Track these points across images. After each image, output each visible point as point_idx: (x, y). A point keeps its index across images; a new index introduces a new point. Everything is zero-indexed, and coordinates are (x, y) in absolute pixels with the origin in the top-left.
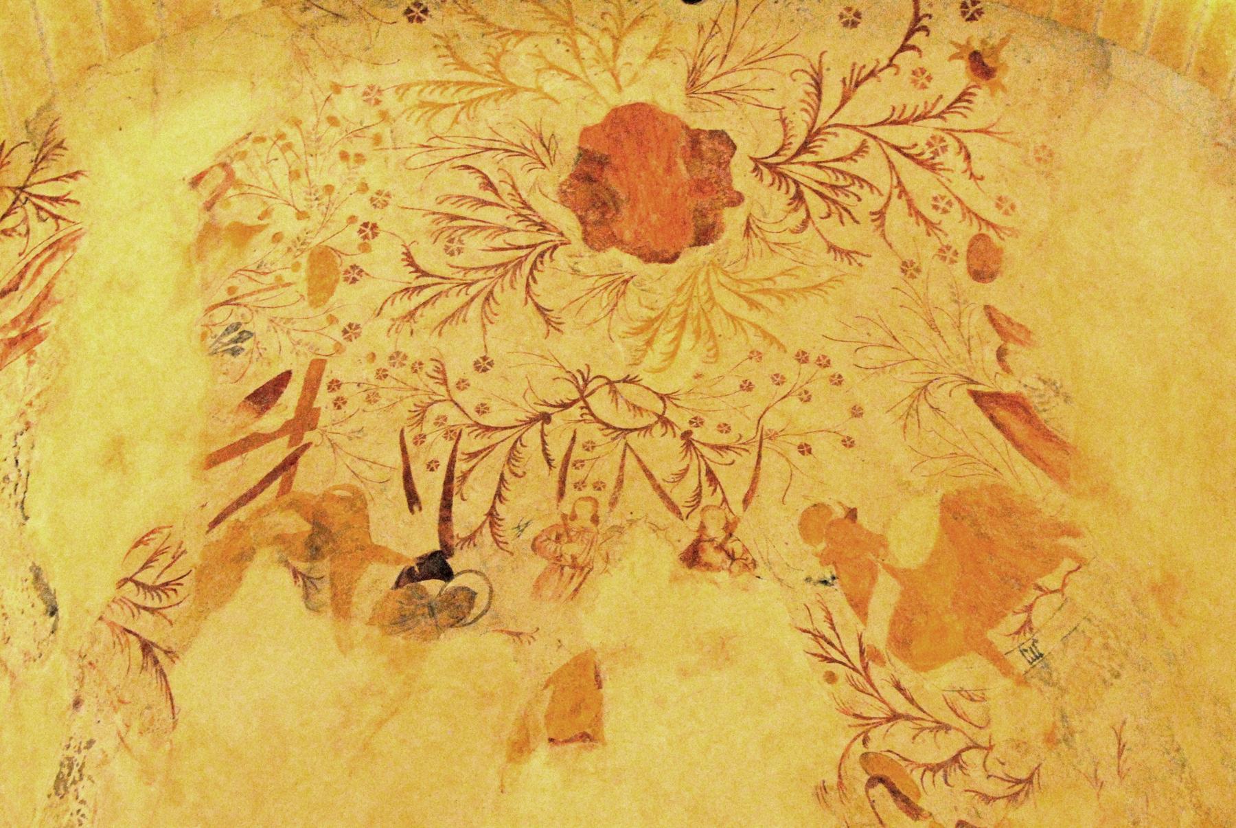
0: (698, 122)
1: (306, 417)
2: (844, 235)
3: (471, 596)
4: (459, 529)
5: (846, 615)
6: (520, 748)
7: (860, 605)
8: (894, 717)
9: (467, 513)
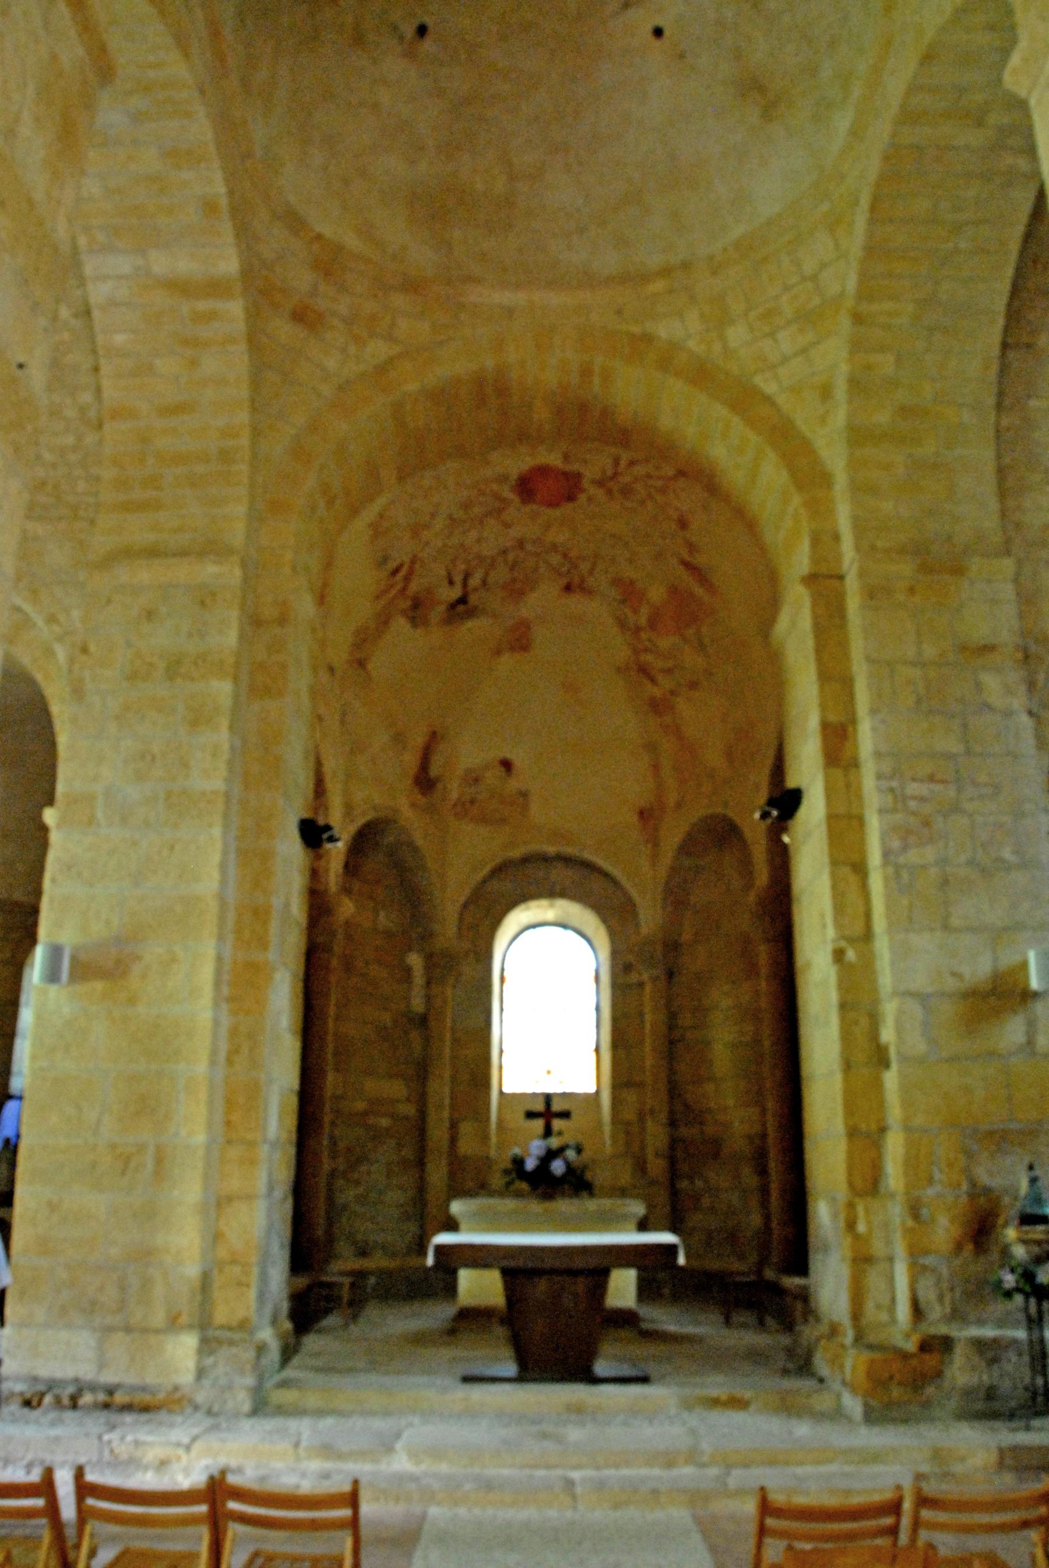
0: (568, 468)
1: (411, 572)
2: (629, 504)
3: (476, 608)
4: (470, 588)
5: (630, 614)
6: (498, 652)
7: (635, 611)
8: (646, 650)
9: (475, 581)
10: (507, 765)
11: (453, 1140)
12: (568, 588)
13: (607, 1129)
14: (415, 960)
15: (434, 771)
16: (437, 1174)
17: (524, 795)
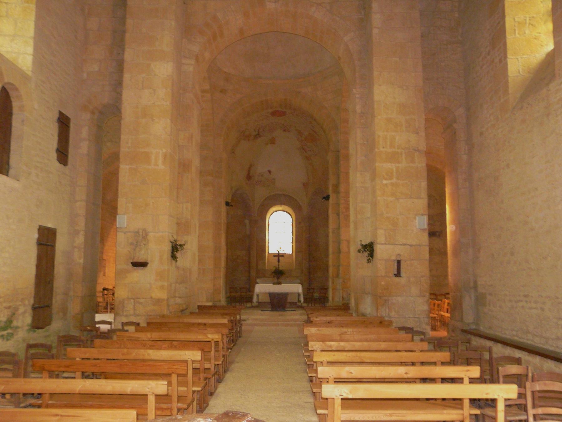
6: (267, 144)
10: (270, 172)
11: (257, 265)
12: (284, 131)
13: (294, 262)
14: (247, 222)
15: (251, 175)
16: (253, 274)
17: (274, 179)
